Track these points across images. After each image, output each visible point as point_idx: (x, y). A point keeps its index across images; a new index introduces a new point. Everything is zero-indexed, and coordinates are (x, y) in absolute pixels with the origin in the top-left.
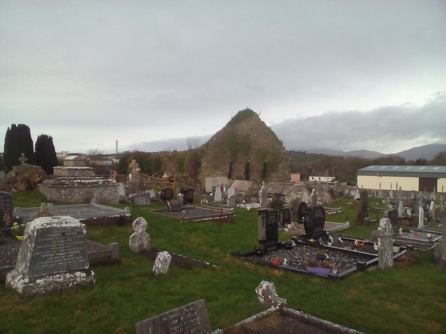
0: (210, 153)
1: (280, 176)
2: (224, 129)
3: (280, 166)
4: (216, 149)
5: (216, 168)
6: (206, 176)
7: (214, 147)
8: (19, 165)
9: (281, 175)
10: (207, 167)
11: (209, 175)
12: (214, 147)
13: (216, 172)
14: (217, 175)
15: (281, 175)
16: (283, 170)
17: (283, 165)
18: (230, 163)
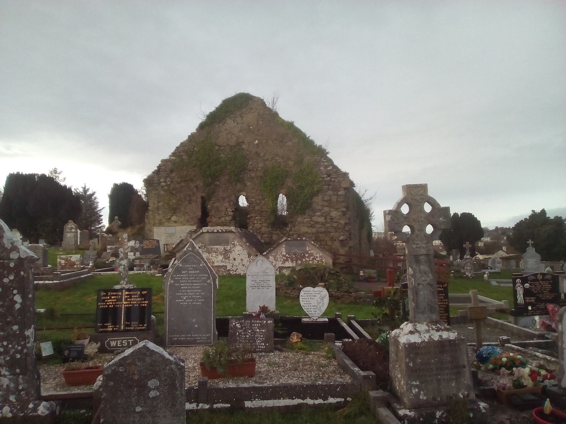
0: (164, 184)
1: (317, 223)
2: (192, 137)
3: (318, 200)
4: (174, 174)
5: (174, 210)
6: (154, 225)
7: (172, 171)
8: (388, 345)
9: (322, 220)
10: (158, 208)
11: (161, 224)
12: (172, 171)
13: (174, 218)
14: (175, 222)
15: (322, 220)
16: (326, 209)
17: (326, 198)
18: (202, 197)
